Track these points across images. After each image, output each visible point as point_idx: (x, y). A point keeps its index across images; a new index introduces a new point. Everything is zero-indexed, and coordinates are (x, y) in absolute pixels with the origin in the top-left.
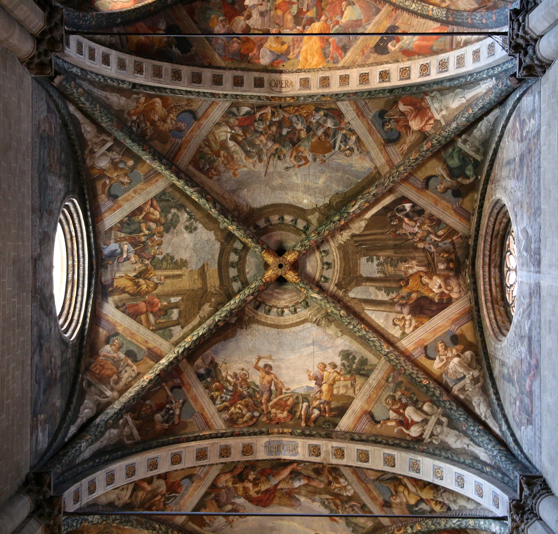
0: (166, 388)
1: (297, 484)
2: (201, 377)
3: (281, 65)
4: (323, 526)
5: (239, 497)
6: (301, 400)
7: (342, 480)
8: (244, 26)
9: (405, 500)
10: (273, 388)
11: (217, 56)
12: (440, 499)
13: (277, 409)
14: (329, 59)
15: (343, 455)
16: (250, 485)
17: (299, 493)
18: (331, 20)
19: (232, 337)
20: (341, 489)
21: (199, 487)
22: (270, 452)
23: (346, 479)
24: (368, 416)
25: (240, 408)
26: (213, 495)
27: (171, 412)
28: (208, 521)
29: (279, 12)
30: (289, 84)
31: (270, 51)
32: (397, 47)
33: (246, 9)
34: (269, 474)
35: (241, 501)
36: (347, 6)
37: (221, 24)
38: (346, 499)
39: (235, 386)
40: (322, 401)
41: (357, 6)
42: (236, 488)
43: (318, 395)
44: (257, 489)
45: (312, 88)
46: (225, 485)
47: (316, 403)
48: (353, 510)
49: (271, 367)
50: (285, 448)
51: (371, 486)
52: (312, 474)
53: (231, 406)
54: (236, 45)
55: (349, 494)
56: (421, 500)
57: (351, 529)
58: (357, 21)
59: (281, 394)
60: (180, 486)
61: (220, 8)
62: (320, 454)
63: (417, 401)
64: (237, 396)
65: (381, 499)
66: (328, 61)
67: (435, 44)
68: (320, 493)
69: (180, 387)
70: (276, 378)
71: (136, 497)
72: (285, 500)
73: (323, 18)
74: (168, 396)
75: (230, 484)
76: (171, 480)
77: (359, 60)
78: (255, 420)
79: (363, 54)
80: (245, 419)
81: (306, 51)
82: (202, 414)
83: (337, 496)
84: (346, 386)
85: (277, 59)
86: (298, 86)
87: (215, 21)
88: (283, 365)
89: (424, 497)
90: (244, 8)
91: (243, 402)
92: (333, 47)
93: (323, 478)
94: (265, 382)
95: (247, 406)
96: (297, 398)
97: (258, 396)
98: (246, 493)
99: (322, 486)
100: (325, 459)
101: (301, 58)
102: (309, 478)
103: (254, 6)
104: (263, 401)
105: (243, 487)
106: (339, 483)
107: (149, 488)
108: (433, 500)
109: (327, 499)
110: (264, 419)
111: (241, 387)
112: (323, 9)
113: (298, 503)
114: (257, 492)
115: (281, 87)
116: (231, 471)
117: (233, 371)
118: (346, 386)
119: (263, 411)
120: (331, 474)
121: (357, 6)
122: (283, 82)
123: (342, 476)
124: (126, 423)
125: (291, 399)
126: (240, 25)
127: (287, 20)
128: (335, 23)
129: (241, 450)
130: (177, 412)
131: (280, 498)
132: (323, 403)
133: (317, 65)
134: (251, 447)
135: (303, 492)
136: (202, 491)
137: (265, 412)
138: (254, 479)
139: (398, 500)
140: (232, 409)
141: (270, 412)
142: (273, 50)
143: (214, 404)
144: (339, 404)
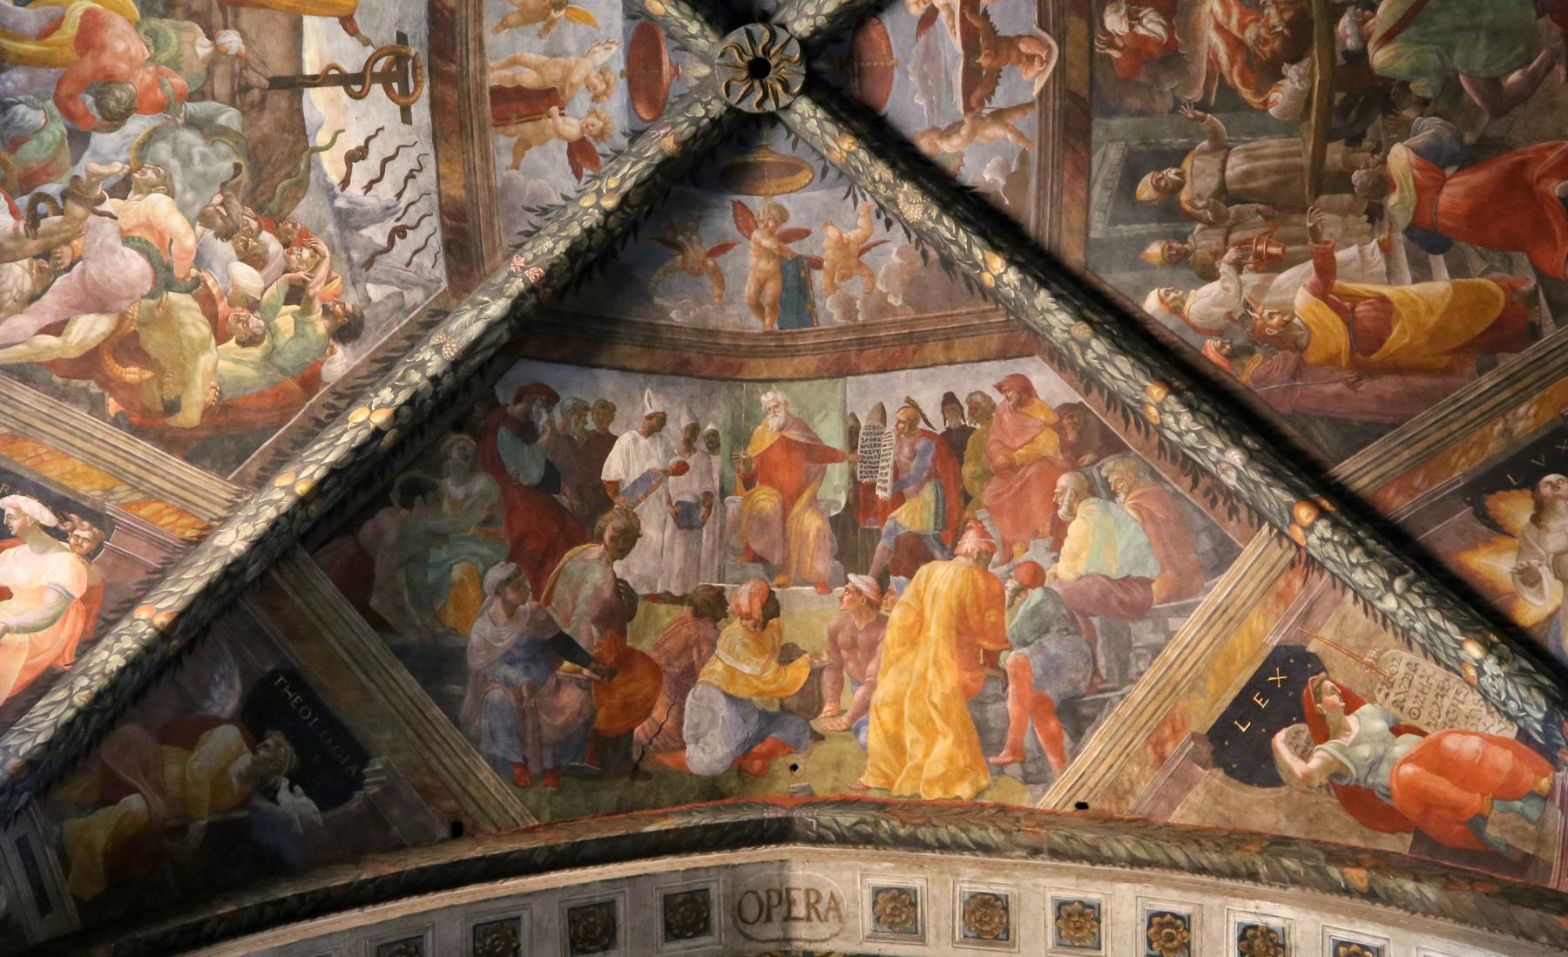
3: (781, 764)
8: (607, 593)
11: (486, 773)
14: (1004, 756)
18: (1008, 558)
29: (766, 499)
30: (825, 907)
31: (732, 699)
32: (1314, 762)
33: (608, 504)
36: (1078, 497)
37: (497, 607)
41: (1124, 507)
45: (931, 936)
54: (571, 698)
58: (1126, 582)
61: (489, 521)
66: (1001, 769)
67: (1494, 815)
73: (970, 542)
77: (1142, 788)
79: (1162, 758)
81: (897, 702)
85: (760, 737)
86: (864, 918)
87: (472, 592)
90: (601, 496)
92: (1020, 699)
101: (873, 736)
103: (648, 482)
112: (967, 498)
115: (788, 918)
121: (1124, 507)
122: (798, 896)
126: (587, 591)
127: (803, 537)
128: (1024, 573)
133: (946, 780)
142: (742, 692)
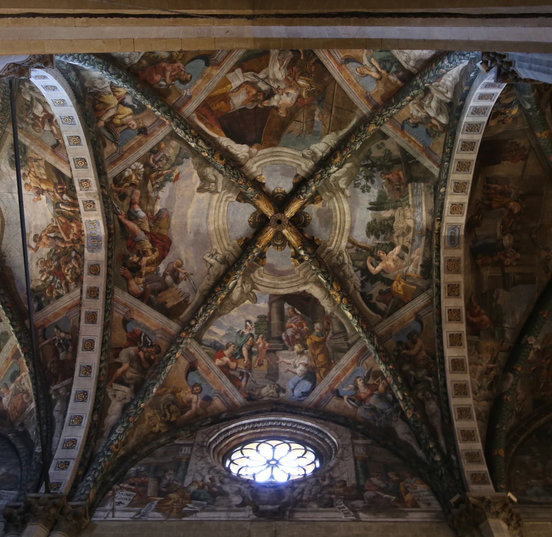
0: (43, 344)
1: (142, 214)
2: (40, 307)
4: (187, 186)
5: (157, 270)
6: (59, 210)
7: (127, 174)
9: (131, 117)
10: (52, 235)
12: (109, 89)
13: (70, 232)
15: (86, 180)
16: (145, 260)
17: (152, 212)
19: (12, 272)
20: (137, 174)
21: (139, 312)
22: (98, 247)
23: (125, 170)
24: (56, 150)
25: (68, 270)
26: (152, 296)
27: (61, 341)
28: (182, 299)
34: (134, 241)
35: (162, 268)
38: (148, 169)
39: (50, 273)
40: (55, 190)
42: (147, 273)
43: (52, 194)
44: (150, 252)
46: (142, 285)
47: (58, 197)
48: (160, 160)
49: (36, 235)
50: (93, 232)
51: (125, 148)
52: (127, 201)
53: (65, 278)
55: (142, 166)
56: (122, 102)
57: (185, 160)
59: (57, 227)
60: (134, 332)
62: (90, 201)
63: (26, 104)
64: (58, 273)
65: (139, 138)
68: (148, 192)
69: (45, 330)
70: (44, 231)
71: (131, 379)
72: (163, 223)
74: (49, 343)
75: (141, 280)
76: (125, 342)
78: (78, 256)
80: (77, 266)
82: (69, 309)
83: (146, 177)
84: (38, 166)
88: (34, 223)
89: (117, 102)
91: (63, 266)
93: (129, 192)
94: (48, 242)
95: (66, 263)
96: (58, 213)
97: (59, 251)
98: (153, 263)
99: (138, 191)
100: (95, 197)
102: (132, 204)
104: (63, 246)
105: (147, 266)
106: (130, 177)
107: (126, 366)
108: (115, 95)
109: (153, 185)
110: (78, 246)
111: (51, 267)
113: (164, 211)
114: (154, 251)
116: (127, 280)
117: (38, 274)
118: (38, 166)
119: (71, 247)
120: (122, 184)
123: (121, 174)
124: (56, 390)
125: (60, 218)
129: (93, 277)
130: (63, 335)
131: (160, 228)
132: (57, 190)
134: (92, 266)
135: (149, 208)
136: (145, 308)
137: (72, 245)
138: (138, 256)
139: (133, 122)
140: (68, 278)
141: (73, 240)
143: (62, 296)
144: (53, 174)
